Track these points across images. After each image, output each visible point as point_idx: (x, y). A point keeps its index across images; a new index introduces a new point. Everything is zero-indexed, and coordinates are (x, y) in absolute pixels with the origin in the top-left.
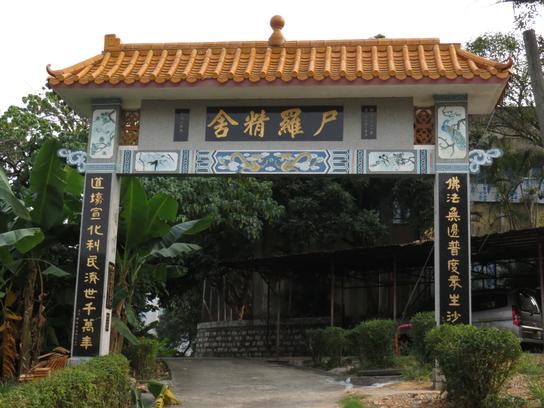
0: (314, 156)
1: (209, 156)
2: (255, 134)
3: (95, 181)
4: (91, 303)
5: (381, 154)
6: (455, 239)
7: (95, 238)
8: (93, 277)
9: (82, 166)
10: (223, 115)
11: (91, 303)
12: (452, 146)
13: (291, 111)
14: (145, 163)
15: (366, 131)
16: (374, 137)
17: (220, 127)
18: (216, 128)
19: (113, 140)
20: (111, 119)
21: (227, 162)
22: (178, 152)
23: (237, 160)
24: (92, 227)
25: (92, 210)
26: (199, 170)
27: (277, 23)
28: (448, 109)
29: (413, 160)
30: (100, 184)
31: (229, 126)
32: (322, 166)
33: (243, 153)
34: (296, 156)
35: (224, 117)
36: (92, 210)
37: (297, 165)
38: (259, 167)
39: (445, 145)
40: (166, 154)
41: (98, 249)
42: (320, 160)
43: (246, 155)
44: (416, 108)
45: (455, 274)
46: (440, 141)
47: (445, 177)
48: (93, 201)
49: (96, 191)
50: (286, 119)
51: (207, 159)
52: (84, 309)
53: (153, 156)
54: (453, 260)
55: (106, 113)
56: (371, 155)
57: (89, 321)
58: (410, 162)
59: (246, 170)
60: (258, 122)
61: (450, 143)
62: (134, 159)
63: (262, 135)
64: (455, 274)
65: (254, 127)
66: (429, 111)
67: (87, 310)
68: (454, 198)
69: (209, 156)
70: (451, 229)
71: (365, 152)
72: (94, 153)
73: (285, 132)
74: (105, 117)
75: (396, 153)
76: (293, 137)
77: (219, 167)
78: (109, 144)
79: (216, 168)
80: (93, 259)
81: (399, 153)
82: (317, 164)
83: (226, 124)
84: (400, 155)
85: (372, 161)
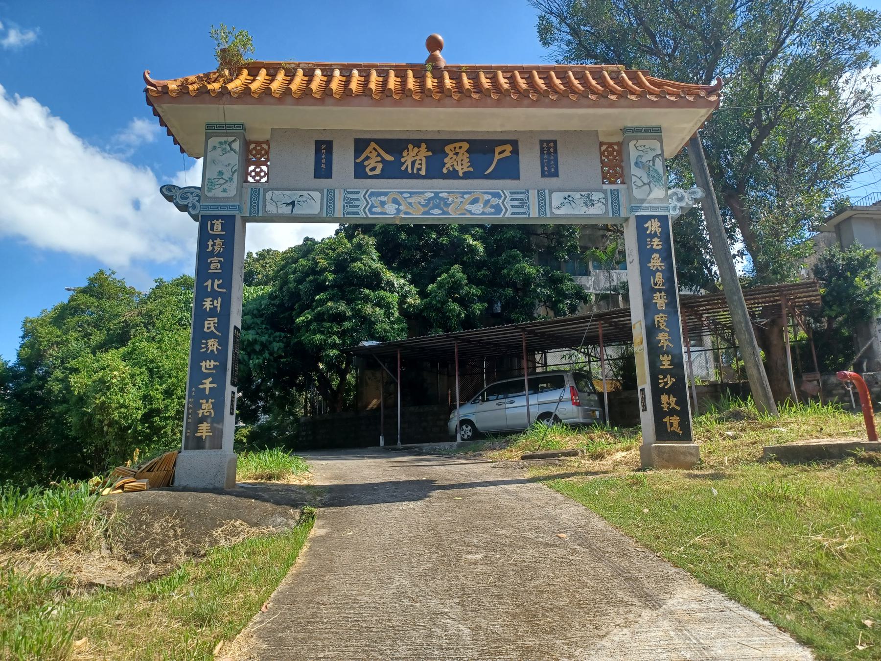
0: (487, 197)
1: (361, 196)
2: (415, 172)
3: (213, 225)
4: (210, 379)
5: (566, 194)
6: (660, 291)
7: (214, 295)
8: (213, 345)
9: (194, 207)
10: (374, 149)
11: (210, 379)
12: (649, 184)
13: (457, 145)
14: (279, 204)
15: (546, 169)
16: (556, 175)
17: (371, 163)
18: (366, 163)
19: (236, 175)
20: (232, 149)
21: (383, 204)
22: (321, 191)
23: (395, 201)
24: (210, 281)
25: (209, 260)
26: (348, 213)
27: (434, 44)
28: (641, 143)
29: (603, 201)
30: (220, 229)
31: (383, 161)
32: (498, 209)
33: (402, 193)
34: (465, 196)
35: (376, 150)
36: (209, 260)
37: (468, 207)
38: (423, 209)
39: (641, 184)
40: (305, 193)
41: (219, 309)
42: (495, 201)
43: (406, 195)
44: (601, 144)
45: (663, 330)
46: (634, 179)
47: (641, 220)
48: (210, 248)
49: (214, 237)
50: (451, 154)
51: (358, 200)
52: (201, 386)
53: (289, 196)
54: (661, 315)
55: (225, 142)
56: (555, 195)
57: (207, 402)
58: (600, 204)
59: (406, 213)
60: (418, 158)
61: (646, 181)
62: (264, 199)
63: (423, 173)
64: (663, 330)
65: (413, 163)
66: (616, 147)
67: (205, 389)
68: (655, 244)
69: (361, 196)
70: (654, 278)
71: (547, 192)
72: (210, 190)
73: (451, 169)
74: (224, 146)
75: (583, 193)
76: (461, 175)
77: (374, 210)
78: (231, 179)
79: (370, 210)
80: (212, 322)
81: (586, 193)
82: (492, 207)
83: (379, 159)
84: (588, 196)
85: (555, 203)
